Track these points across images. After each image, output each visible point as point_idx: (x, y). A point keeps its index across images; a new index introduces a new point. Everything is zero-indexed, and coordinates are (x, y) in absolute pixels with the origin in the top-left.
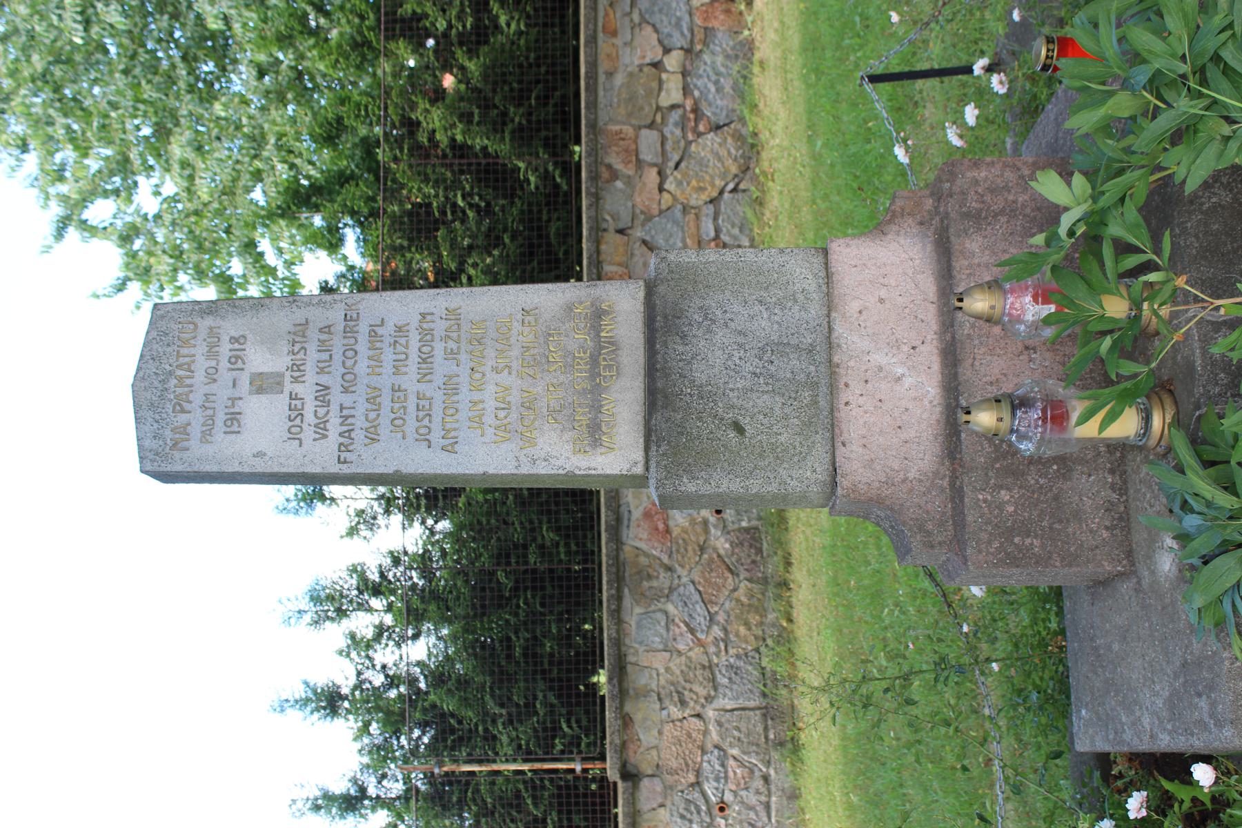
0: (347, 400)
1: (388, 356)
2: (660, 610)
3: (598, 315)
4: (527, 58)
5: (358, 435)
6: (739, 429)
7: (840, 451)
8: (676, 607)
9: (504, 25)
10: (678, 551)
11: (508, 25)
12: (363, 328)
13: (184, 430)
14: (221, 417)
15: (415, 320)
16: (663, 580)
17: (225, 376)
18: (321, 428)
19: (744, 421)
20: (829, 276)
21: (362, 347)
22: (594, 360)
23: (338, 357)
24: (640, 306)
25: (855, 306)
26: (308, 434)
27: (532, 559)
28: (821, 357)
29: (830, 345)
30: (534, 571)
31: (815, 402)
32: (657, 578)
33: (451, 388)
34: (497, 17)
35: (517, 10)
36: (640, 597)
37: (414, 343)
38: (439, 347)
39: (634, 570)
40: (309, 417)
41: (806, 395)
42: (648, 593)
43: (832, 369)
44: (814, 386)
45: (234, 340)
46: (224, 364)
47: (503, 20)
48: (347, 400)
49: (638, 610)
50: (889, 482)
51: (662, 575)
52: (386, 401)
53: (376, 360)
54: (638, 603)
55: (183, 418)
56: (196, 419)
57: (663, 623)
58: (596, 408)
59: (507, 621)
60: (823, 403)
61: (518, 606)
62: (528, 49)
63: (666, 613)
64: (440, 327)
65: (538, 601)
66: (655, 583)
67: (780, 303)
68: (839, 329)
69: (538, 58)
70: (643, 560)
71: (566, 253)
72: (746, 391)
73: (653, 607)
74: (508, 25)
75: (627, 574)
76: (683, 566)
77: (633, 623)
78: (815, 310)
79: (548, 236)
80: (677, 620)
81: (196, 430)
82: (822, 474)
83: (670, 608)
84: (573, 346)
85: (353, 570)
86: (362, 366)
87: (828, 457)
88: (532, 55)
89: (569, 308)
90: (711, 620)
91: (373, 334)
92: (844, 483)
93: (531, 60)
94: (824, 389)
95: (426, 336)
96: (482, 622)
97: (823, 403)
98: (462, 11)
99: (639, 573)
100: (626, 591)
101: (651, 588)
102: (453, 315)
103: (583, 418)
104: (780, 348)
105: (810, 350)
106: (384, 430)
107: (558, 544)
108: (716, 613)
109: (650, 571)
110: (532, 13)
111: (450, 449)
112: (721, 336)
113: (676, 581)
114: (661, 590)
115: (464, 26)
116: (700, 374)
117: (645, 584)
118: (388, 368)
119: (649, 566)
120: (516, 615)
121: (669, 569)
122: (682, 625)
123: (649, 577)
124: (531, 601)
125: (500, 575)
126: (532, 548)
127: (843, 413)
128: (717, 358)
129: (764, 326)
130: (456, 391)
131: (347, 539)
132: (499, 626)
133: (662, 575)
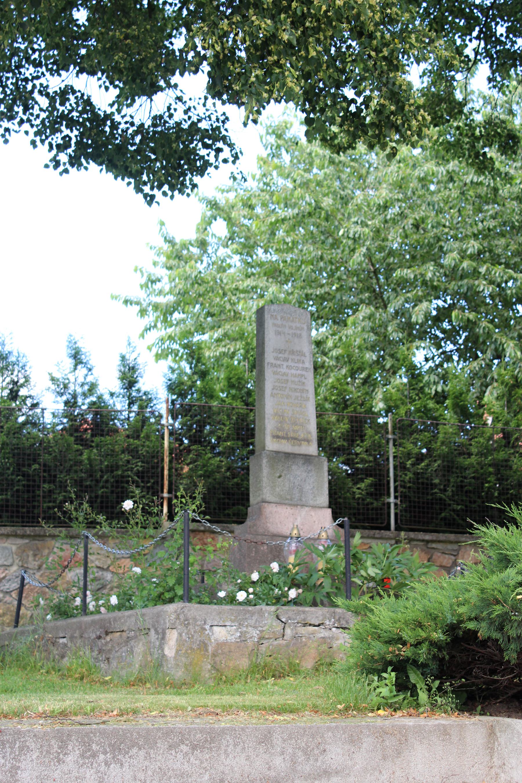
0: (285, 366)
1: (296, 379)
2: (14, 562)
3: (308, 441)
4: (340, 497)
5: (275, 369)
6: (280, 477)
7: (274, 505)
8: (15, 571)
9: (358, 486)
10: (51, 573)
11: (359, 488)
12: (304, 373)
13: (276, 318)
14: (280, 329)
15: (306, 388)
16: (33, 564)
17: (291, 332)
18: (277, 358)
19: (281, 479)
20: (321, 508)
21: (299, 372)
22: (295, 439)
23: (296, 365)
24: (310, 453)
25: (313, 514)
26: (275, 354)
27: (46, 486)
28: (299, 502)
29: (303, 506)
30: (39, 486)
31: (287, 499)
32: (35, 560)
33: (288, 397)
34: (363, 482)
35: (367, 493)
36: (22, 550)
37: (299, 387)
38: (298, 394)
39: (39, 546)
40: (280, 355)
41: (289, 497)
42: (25, 554)
43: (296, 505)
44: (291, 500)
45: (300, 335)
46: (294, 331)
47: (362, 485)
48: (285, 366)
49: (14, 548)
50: (266, 518)
51: (36, 563)
52: (285, 378)
53: (295, 376)
54: (19, 548)
55: (279, 318)
56: (279, 322)
57: (5, 563)
58: (283, 438)
59: (8, 469)
60: (287, 502)
61: (18, 475)
62: (345, 498)
63: (11, 565)
64: (304, 395)
65: (21, 488)
66: (31, 559)
67: (313, 493)
68: (307, 509)
69: (340, 503)
70: (46, 552)
71: (229, 515)
72: (290, 480)
73: (15, 556)
74: (359, 488)
75: (37, 542)
76: (41, 576)
77: (6, 545)
78: (311, 502)
79: (238, 504)
80: (7, 572)
81: (276, 322)
82: (268, 499)
83: (15, 568)
84: (299, 433)
85: (27, 379)
86: (293, 371)
87: (272, 501)
88: (341, 500)
89: (310, 433)
90: (7, 592)
91: (302, 375)
92: (266, 505)
93: (339, 500)
94: (290, 502)
95: (302, 391)
96: (9, 453)
97: (287, 502)
98: (366, 462)
99: (38, 549)
100: (27, 541)
101: (28, 556)
102: (308, 399)
103: (280, 434)
104: (301, 491)
105: (301, 500)
106: (277, 377)
107: (54, 502)
108: (11, 596)
109: (39, 556)
110: (366, 502)
111: (272, 395)
112: (304, 474)
113: (31, 572)
114: (27, 562)
115: (357, 463)
116: (294, 467)
117: (31, 553)
118: (293, 379)
119: (42, 556)
120: (12, 474)
121: (40, 568)
122: (4, 575)
123: (35, 555)
124: (21, 483)
125: (36, 466)
126: (52, 486)
127: (284, 507)
128: (298, 473)
129: (307, 487)
130: (287, 398)
131: (48, 377)
132: (6, 463)
133: (36, 563)
